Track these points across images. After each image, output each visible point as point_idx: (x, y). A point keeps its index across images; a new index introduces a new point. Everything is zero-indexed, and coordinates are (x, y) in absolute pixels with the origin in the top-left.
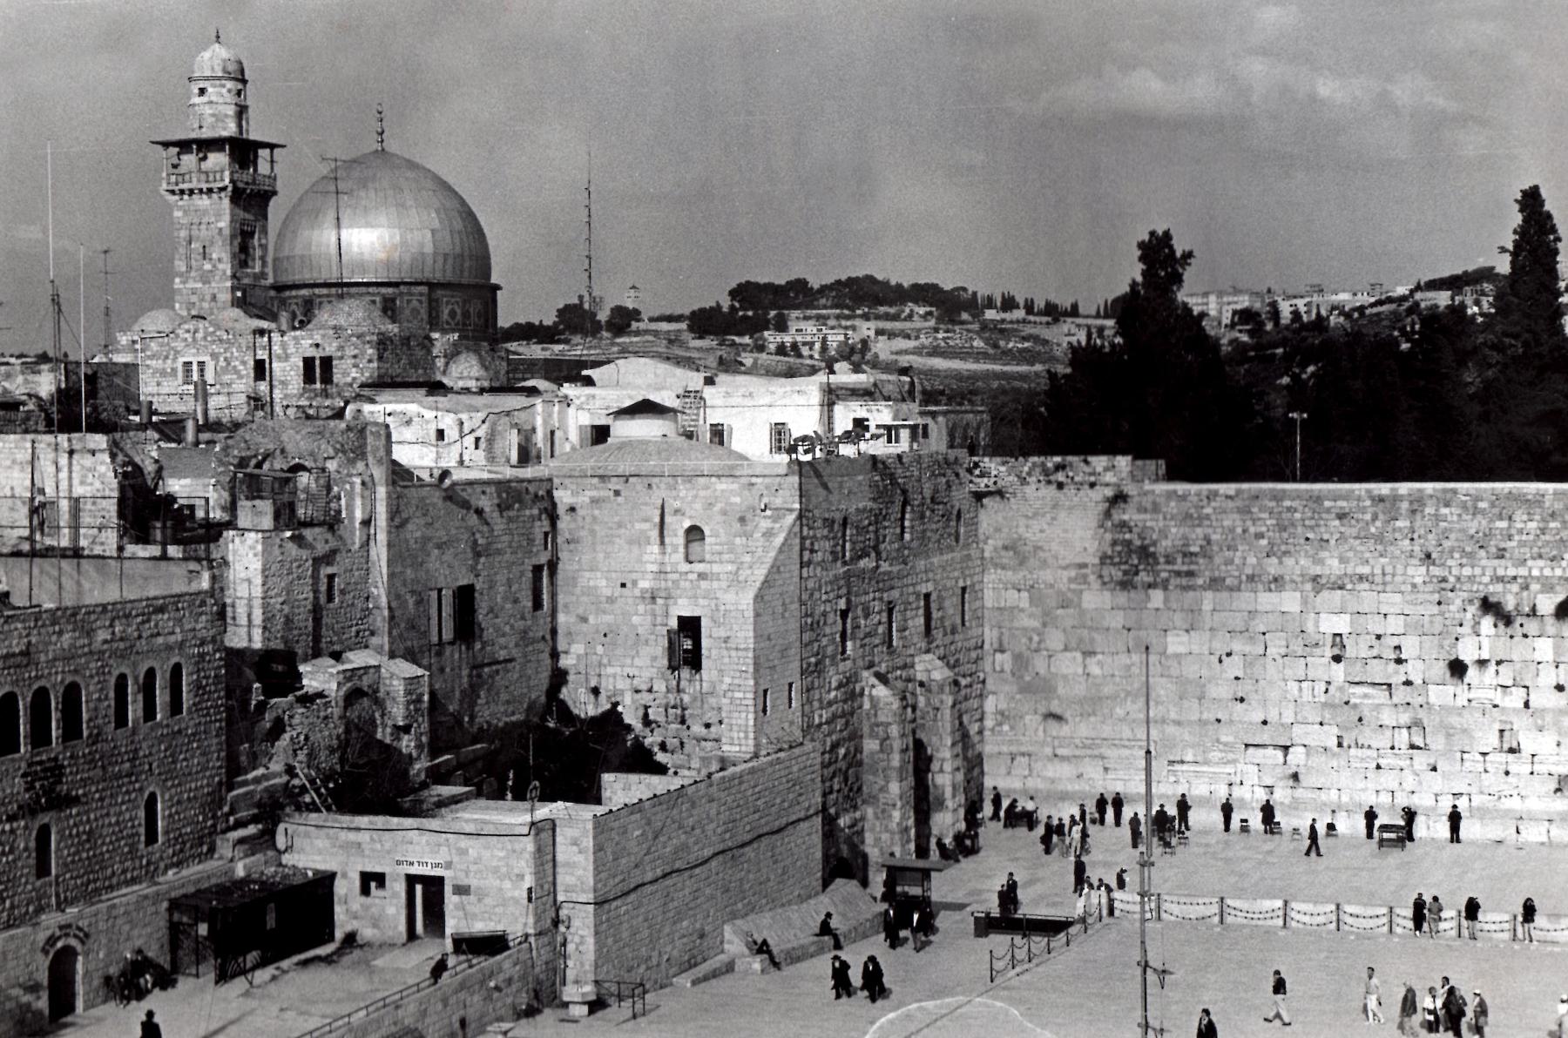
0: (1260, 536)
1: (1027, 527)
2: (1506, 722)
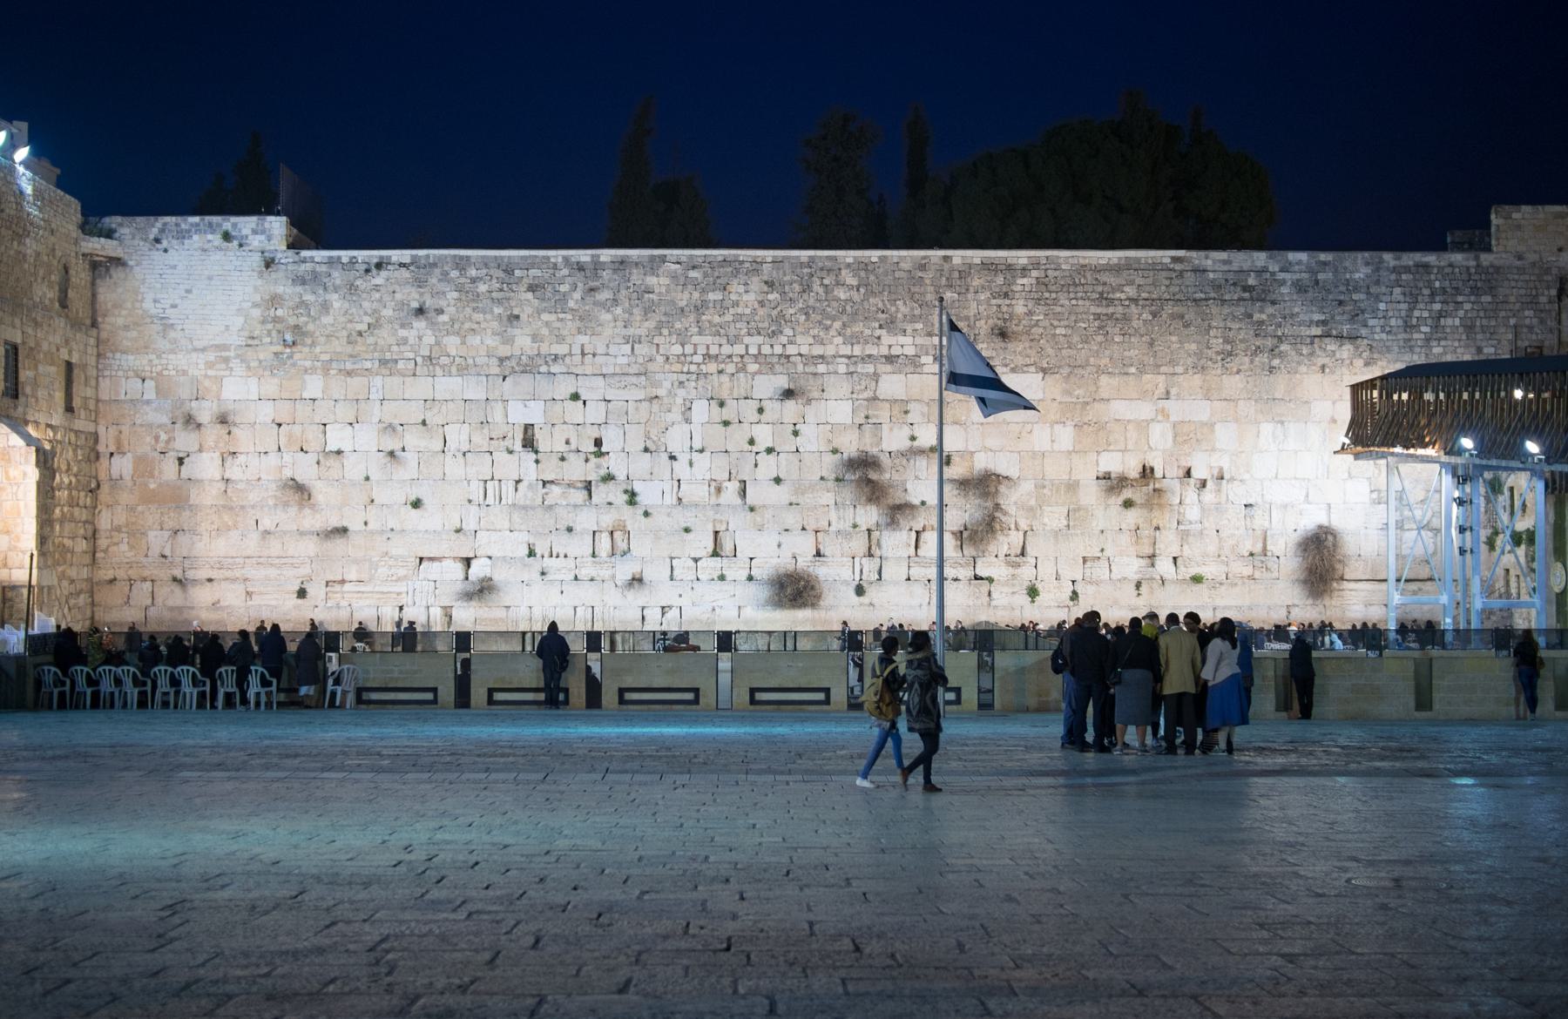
0: (440, 311)
1: (155, 301)
2: (721, 521)
